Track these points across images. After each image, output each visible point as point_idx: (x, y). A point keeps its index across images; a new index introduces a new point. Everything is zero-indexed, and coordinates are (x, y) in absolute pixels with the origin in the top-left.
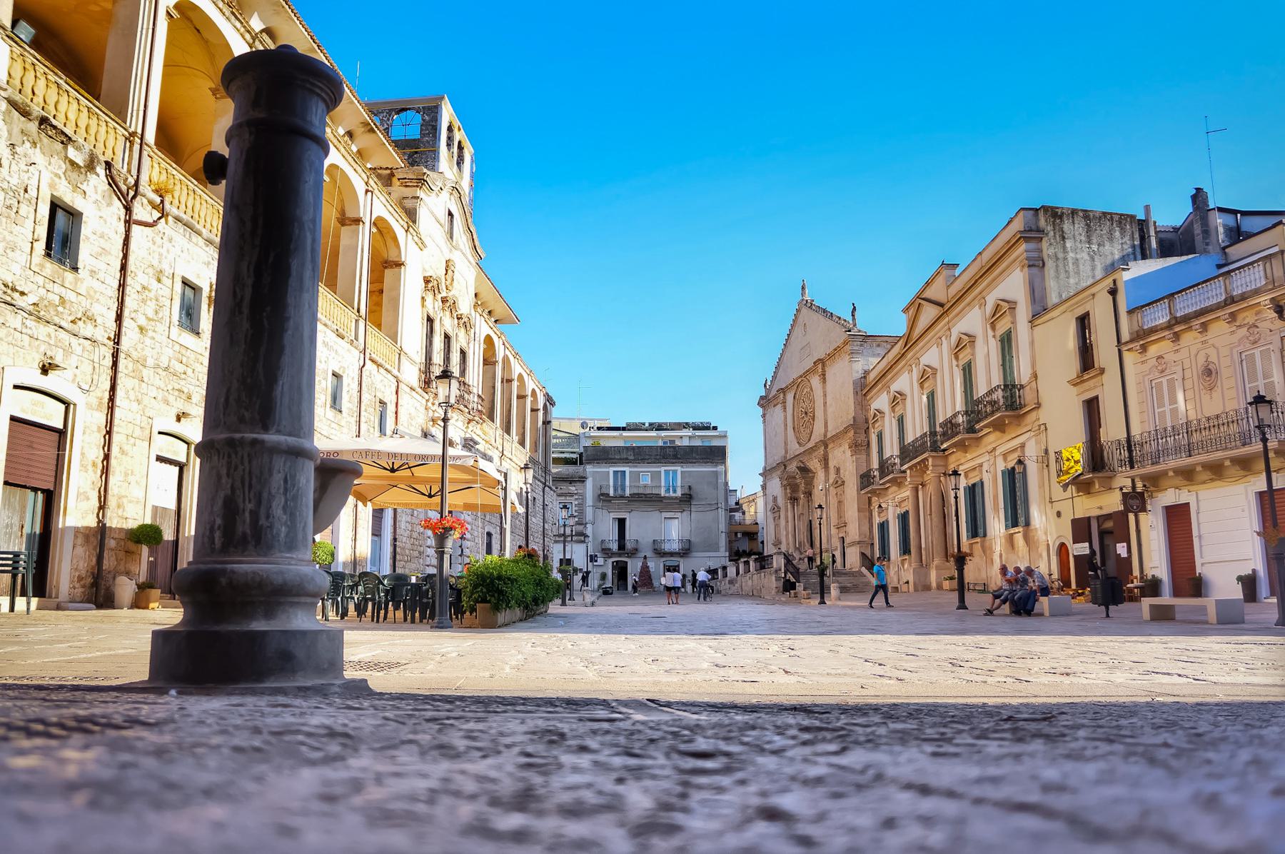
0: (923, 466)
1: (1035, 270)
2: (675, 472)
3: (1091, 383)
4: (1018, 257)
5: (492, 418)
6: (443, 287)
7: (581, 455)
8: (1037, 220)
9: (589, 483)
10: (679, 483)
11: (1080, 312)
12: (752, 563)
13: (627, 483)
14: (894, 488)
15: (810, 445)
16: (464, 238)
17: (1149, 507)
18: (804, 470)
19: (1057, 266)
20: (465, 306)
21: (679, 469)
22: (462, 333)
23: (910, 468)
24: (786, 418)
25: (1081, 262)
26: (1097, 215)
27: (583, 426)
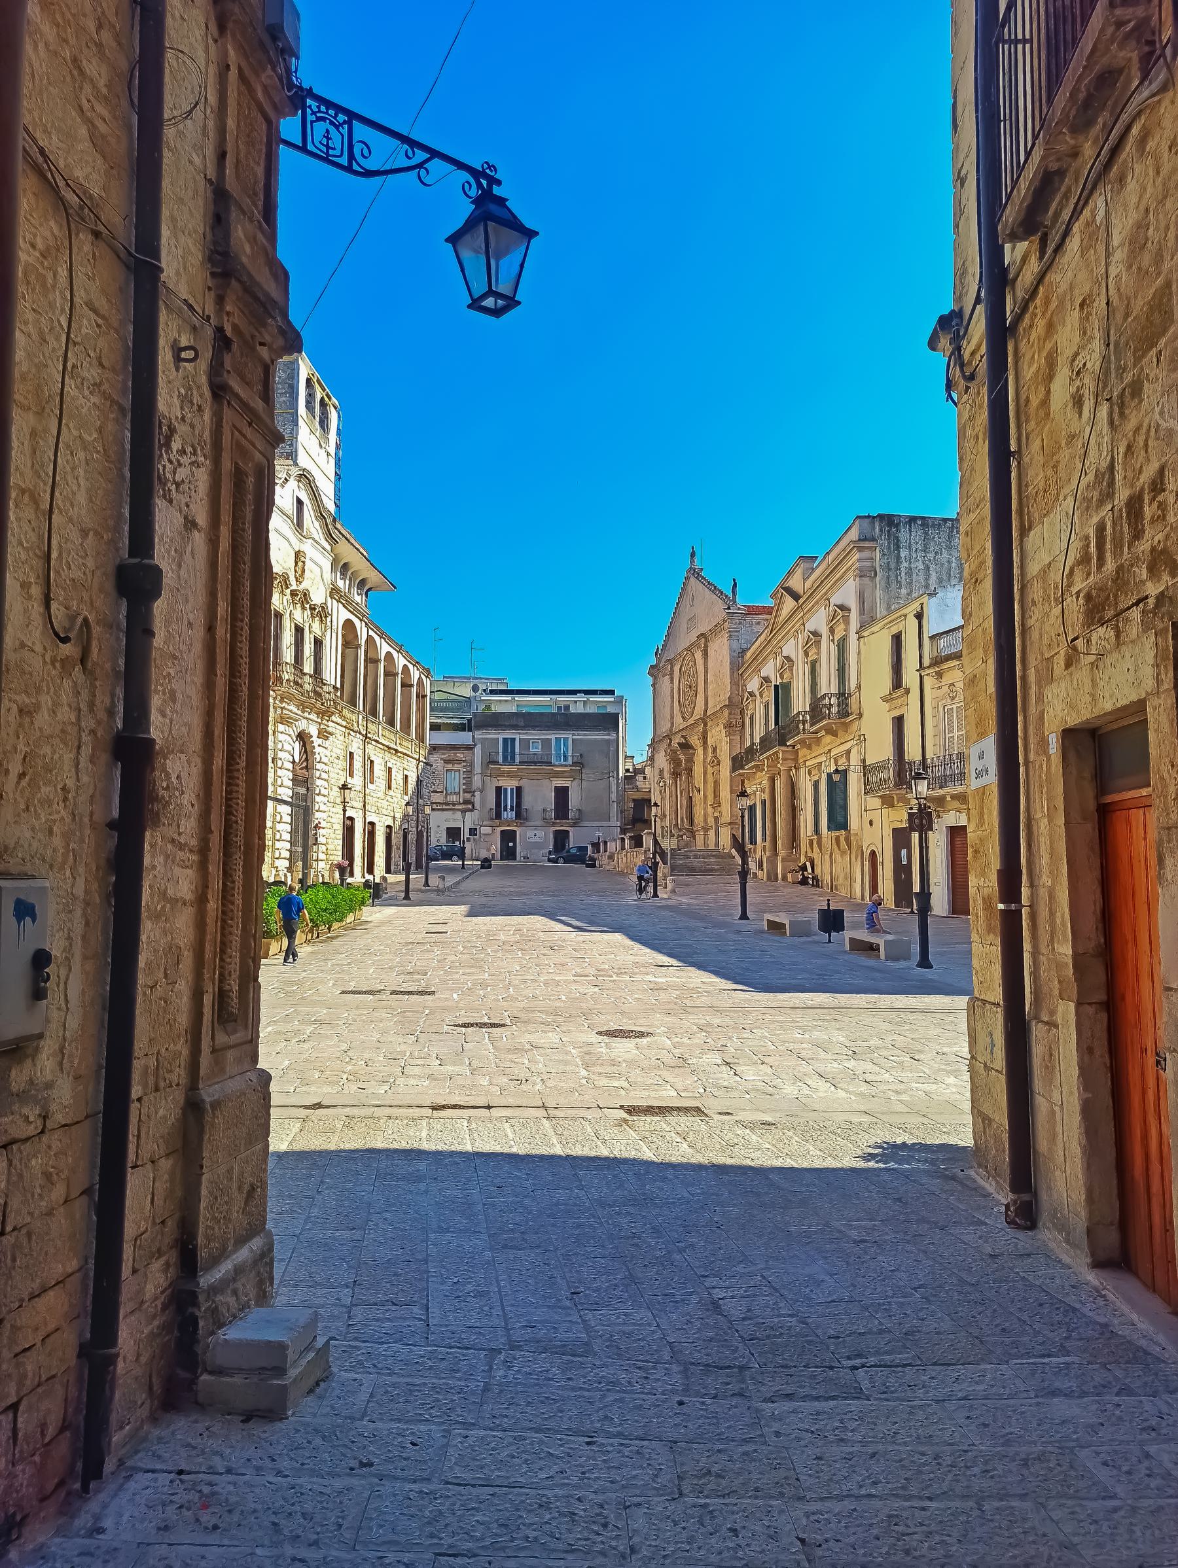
0: (774, 759)
1: (866, 580)
2: (566, 740)
3: (899, 702)
4: (852, 565)
5: (353, 702)
6: (292, 580)
7: (469, 721)
8: (873, 528)
9: (478, 750)
10: (570, 752)
11: (894, 630)
12: (627, 841)
13: (517, 750)
14: (829, 738)
15: (691, 721)
16: (317, 524)
17: (935, 826)
18: (686, 746)
19: (888, 577)
20: (318, 596)
21: (569, 736)
22: (316, 625)
23: (767, 758)
24: (672, 689)
25: (915, 571)
26: (936, 522)
27: (475, 689)
